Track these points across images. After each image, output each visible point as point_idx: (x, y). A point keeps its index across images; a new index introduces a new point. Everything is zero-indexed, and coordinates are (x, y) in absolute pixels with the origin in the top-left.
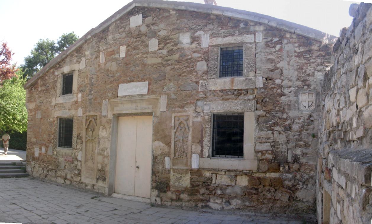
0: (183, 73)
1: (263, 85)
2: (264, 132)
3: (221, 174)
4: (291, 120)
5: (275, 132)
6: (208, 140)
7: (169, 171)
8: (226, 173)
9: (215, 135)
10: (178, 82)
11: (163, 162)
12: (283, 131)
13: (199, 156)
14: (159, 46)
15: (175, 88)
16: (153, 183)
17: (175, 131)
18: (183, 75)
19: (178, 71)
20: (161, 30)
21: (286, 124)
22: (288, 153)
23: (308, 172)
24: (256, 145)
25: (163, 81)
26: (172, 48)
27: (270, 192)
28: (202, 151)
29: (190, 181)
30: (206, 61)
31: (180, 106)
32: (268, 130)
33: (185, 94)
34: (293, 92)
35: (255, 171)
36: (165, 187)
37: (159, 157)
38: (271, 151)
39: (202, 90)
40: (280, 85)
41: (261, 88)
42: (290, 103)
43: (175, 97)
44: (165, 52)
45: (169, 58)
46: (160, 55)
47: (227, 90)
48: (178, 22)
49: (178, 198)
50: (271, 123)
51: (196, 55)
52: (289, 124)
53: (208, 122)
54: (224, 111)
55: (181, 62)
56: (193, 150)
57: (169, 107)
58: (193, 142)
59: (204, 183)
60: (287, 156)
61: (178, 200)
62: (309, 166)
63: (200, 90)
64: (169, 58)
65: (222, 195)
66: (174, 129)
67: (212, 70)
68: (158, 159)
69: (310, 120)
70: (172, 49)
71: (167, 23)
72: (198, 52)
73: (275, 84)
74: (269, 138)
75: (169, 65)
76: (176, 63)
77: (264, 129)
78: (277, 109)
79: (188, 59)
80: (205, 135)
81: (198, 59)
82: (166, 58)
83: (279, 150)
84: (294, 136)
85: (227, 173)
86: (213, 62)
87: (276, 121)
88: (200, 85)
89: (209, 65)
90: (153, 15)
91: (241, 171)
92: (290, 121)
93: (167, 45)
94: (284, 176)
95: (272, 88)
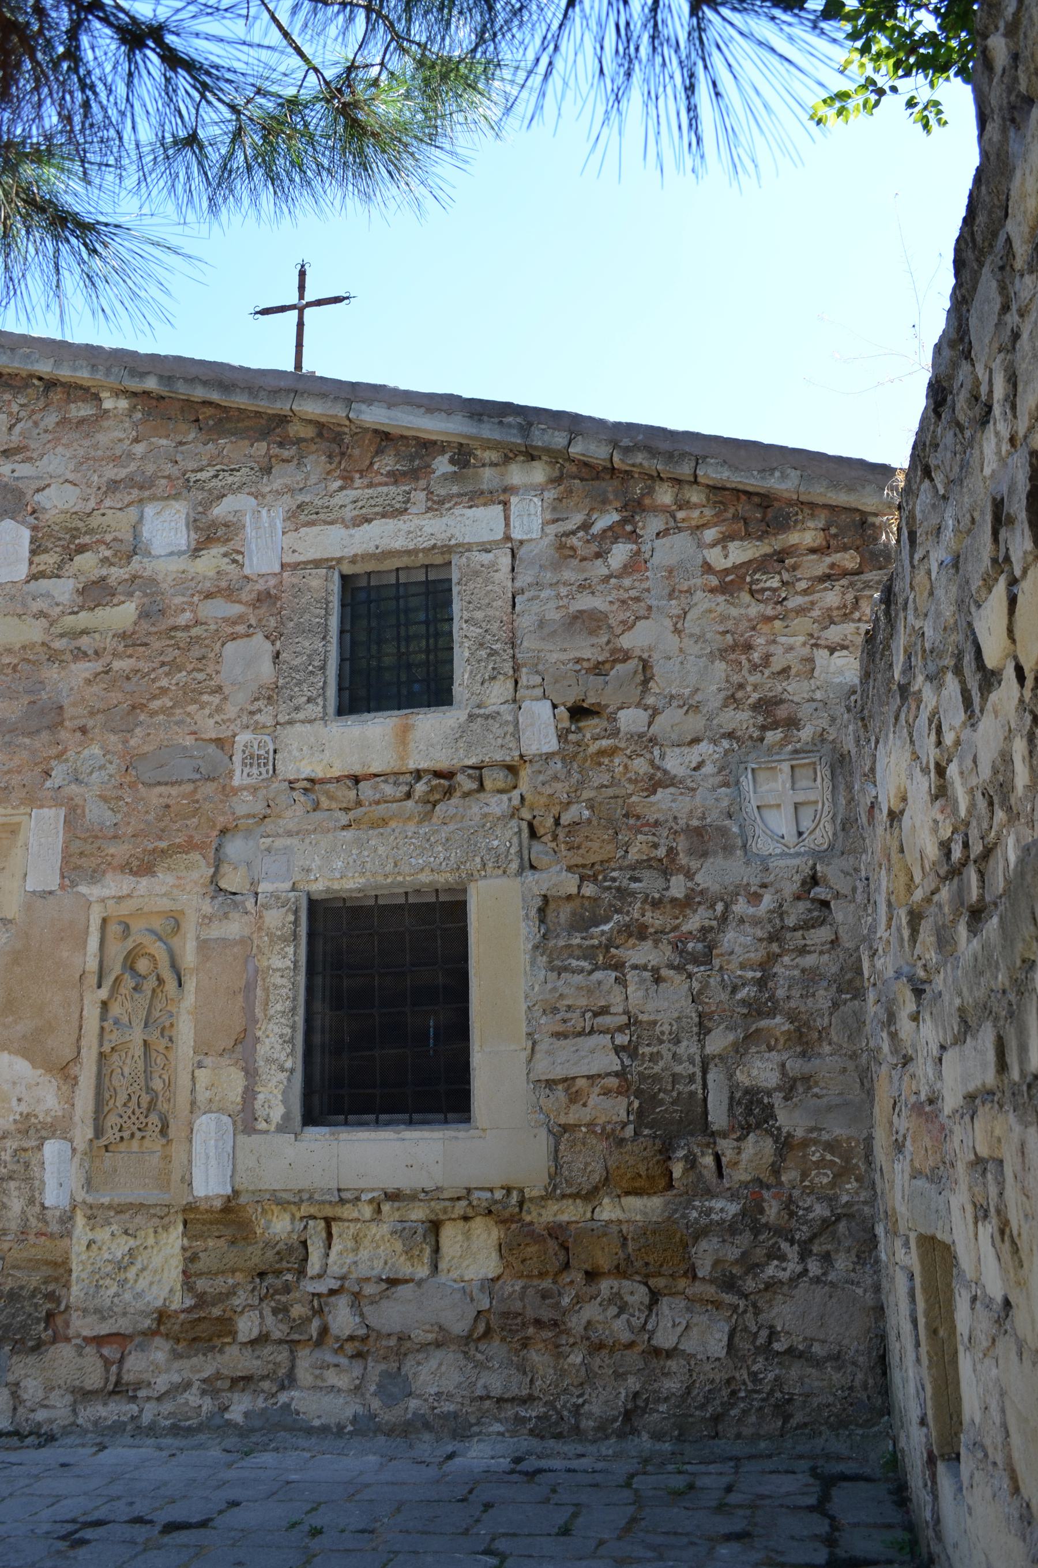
0: (154, 697)
1: (555, 740)
2: (578, 979)
3: (357, 1220)
4: (712, 906)
5: (631, 976)
6: (281, 1036)
7: (67, 1219)
8: (379, 1211)
9: (318, 1006)
10: (125, 742)
12: (671, 966)
13: (234, 1123)
14: (36, 559)
15: (112, 769)
17: (103, 993)
18: (155, 704)
19: (128, 687)
20: (49, 485)
21: (685, 928)
22: (711, 1085)
23: (825, 1181)
24: (537, 1048)
25: (45, 736)
26: (104, 572)
27: (622, 1310)
28: (249, 1094)
29: (184, 1272)
30: (267, 637)
31: (135, 863)
32: (596, 968)
33: (163, 801)
34: (708, 769)
35: (535, 1193)
36: (38, 1320)
38: (617, 1074)
39: (247, 781)
40: (641, 736)
41: (548, 757)
42: (704, 818)
43: (109, 818)
44: (63, 590)
45: (84, 619)
46: (36, 606)
47: (376, 775)
48: (139, 449)
49: (113, 1379)
50: (606, 928)
51: (220, 609)
52: (704, 930)
53: (284, 939)
54: (362, 880)
55: (146, 645)
56: (203, 1096)
57: (77, 868)
58: (202, 1049)
59: (262, 1275)
60: (705, 1100)
61: (113, 1392)
62: (831, 1146)
63: (236, 782)
64: (84, 619)
65: (364, 1339)
66: (99, 986)
67: (299, 683)
69: (813, 901)
70: (103, 579)
71: (81, 452)
72: (229, 593)
73: (616, 733)
74: (604, 1011)
75: (80, 654)
76: (121, 648)
77: (574, 963)
78: (633, 855)
79: (175, 628)
80: (265, 1010)
81: (230, 630)
82: (69, 620)
83: (657, 1069)
84: (735, 990)
85: (386, 1207)
86: (307, 644)
87: (636, 915)
88: (237, 758)
89: (284, 656)
90: (15, 408)
91: (464, 1193)
92: (709, 913)
93: (78, 559)
94: (695, 1214)
95: (601, 753)
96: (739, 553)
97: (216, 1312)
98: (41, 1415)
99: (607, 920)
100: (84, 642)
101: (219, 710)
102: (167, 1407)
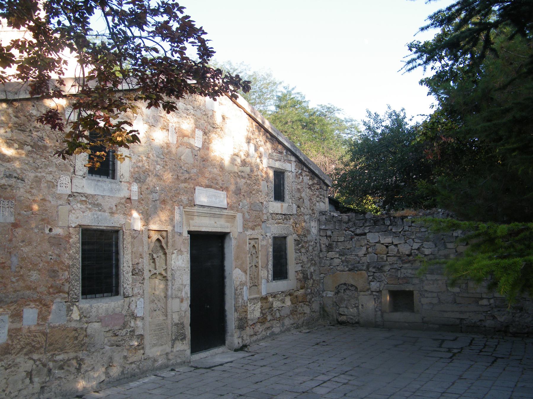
7: (247, 302)
11: (241, 294)
16: (236, 321)
18: (253, 192)
28: (268, 276)
37: (239, 288)
68: (239, 290)
96: (311, 183)
97: (265, 316)
98: (246, 342)
99: (300, 244)
100: (243, 174)
101: (261, 196)
102: (261, 335)
